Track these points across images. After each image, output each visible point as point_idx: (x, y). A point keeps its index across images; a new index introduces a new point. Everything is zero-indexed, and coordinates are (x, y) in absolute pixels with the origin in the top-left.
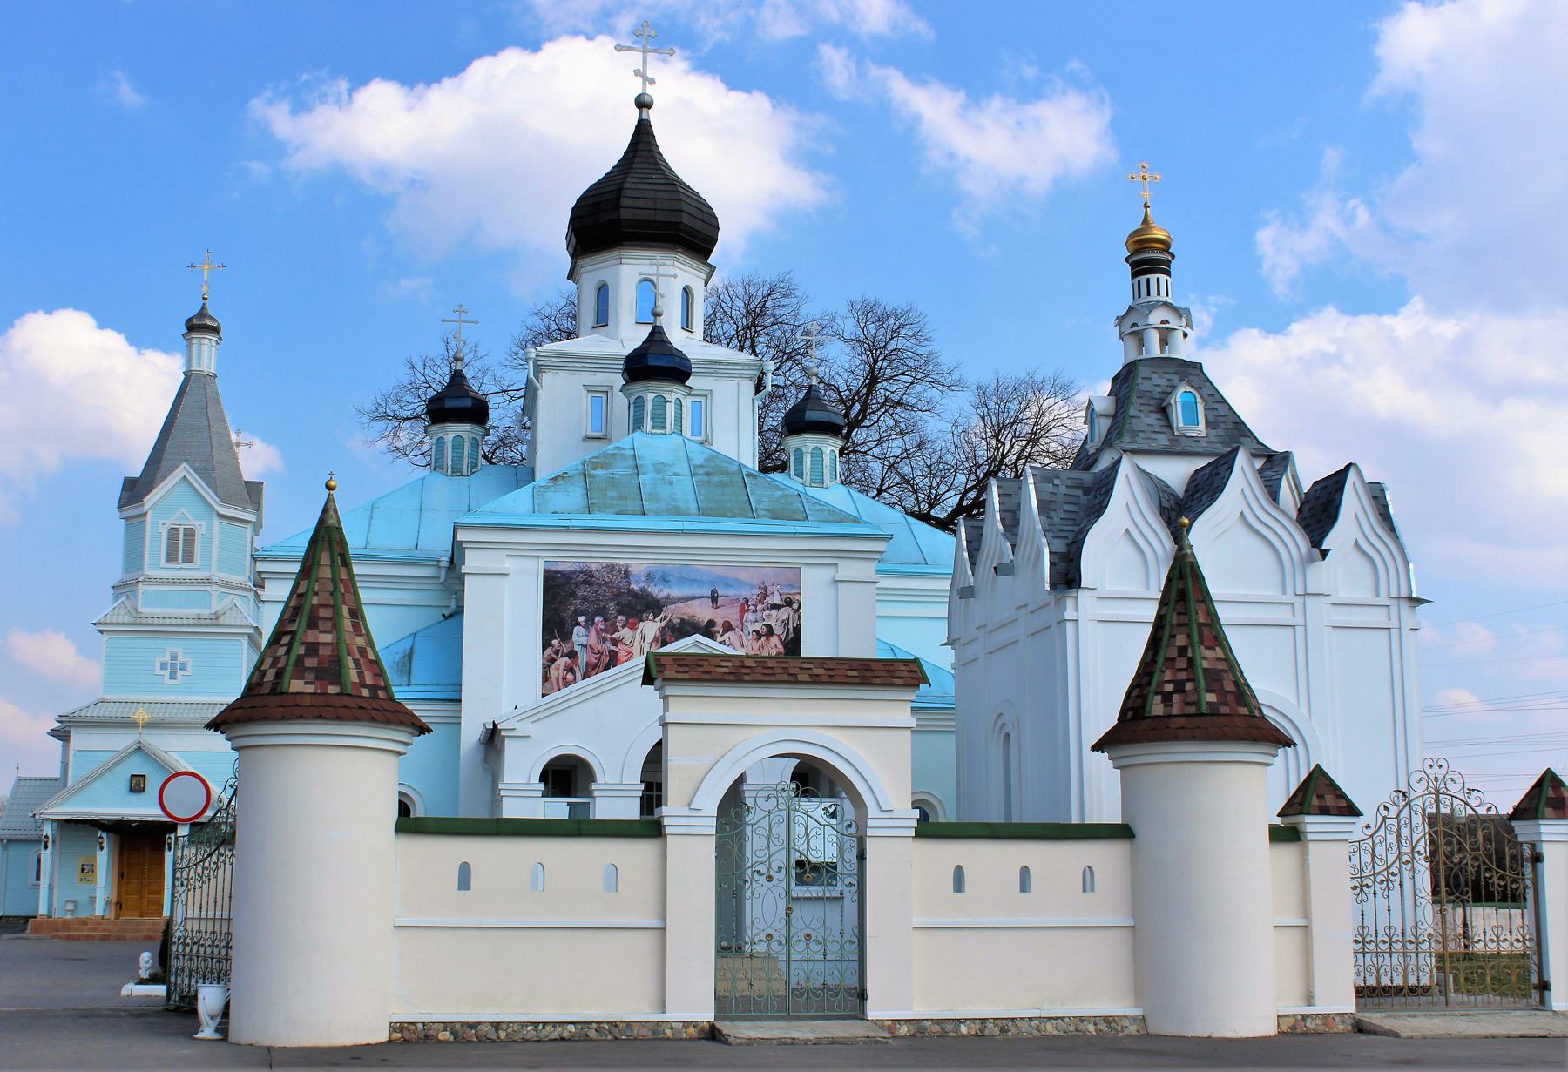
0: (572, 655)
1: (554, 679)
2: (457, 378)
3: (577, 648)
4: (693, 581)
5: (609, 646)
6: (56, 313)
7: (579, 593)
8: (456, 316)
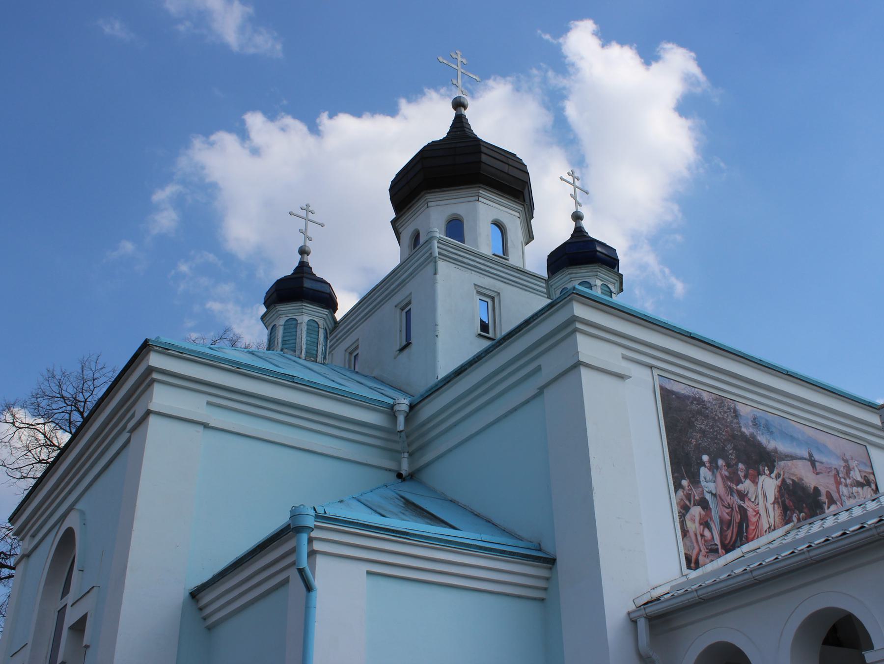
0: (703, 504)
1: (692, 534)
2: (303, 269)
3: (708, 497)
4: (792, 438)
5: (736, 499)
6: (571, 58)
7: (698, 425)
8: (303, 213)
